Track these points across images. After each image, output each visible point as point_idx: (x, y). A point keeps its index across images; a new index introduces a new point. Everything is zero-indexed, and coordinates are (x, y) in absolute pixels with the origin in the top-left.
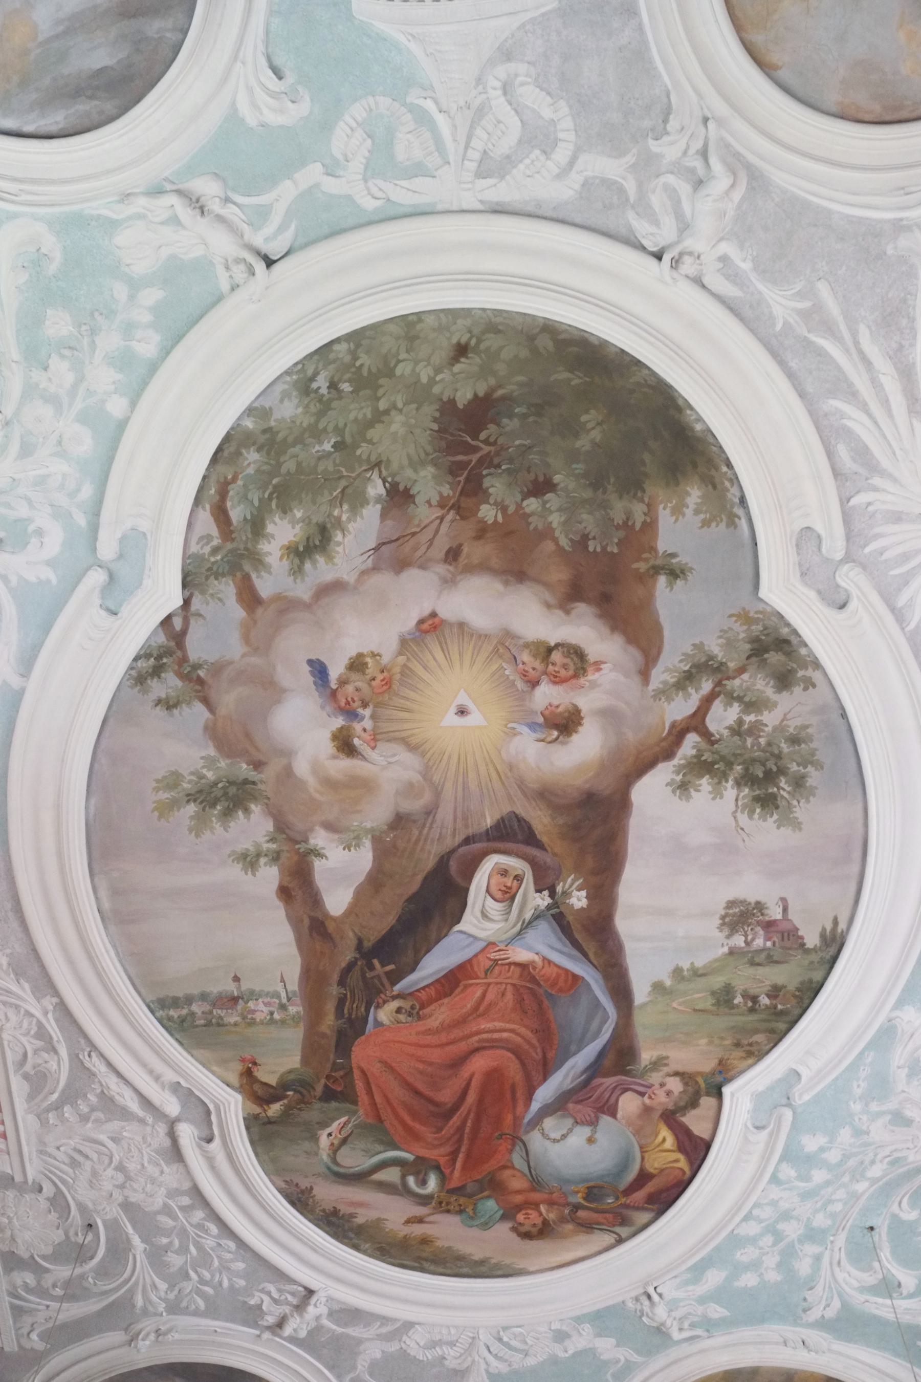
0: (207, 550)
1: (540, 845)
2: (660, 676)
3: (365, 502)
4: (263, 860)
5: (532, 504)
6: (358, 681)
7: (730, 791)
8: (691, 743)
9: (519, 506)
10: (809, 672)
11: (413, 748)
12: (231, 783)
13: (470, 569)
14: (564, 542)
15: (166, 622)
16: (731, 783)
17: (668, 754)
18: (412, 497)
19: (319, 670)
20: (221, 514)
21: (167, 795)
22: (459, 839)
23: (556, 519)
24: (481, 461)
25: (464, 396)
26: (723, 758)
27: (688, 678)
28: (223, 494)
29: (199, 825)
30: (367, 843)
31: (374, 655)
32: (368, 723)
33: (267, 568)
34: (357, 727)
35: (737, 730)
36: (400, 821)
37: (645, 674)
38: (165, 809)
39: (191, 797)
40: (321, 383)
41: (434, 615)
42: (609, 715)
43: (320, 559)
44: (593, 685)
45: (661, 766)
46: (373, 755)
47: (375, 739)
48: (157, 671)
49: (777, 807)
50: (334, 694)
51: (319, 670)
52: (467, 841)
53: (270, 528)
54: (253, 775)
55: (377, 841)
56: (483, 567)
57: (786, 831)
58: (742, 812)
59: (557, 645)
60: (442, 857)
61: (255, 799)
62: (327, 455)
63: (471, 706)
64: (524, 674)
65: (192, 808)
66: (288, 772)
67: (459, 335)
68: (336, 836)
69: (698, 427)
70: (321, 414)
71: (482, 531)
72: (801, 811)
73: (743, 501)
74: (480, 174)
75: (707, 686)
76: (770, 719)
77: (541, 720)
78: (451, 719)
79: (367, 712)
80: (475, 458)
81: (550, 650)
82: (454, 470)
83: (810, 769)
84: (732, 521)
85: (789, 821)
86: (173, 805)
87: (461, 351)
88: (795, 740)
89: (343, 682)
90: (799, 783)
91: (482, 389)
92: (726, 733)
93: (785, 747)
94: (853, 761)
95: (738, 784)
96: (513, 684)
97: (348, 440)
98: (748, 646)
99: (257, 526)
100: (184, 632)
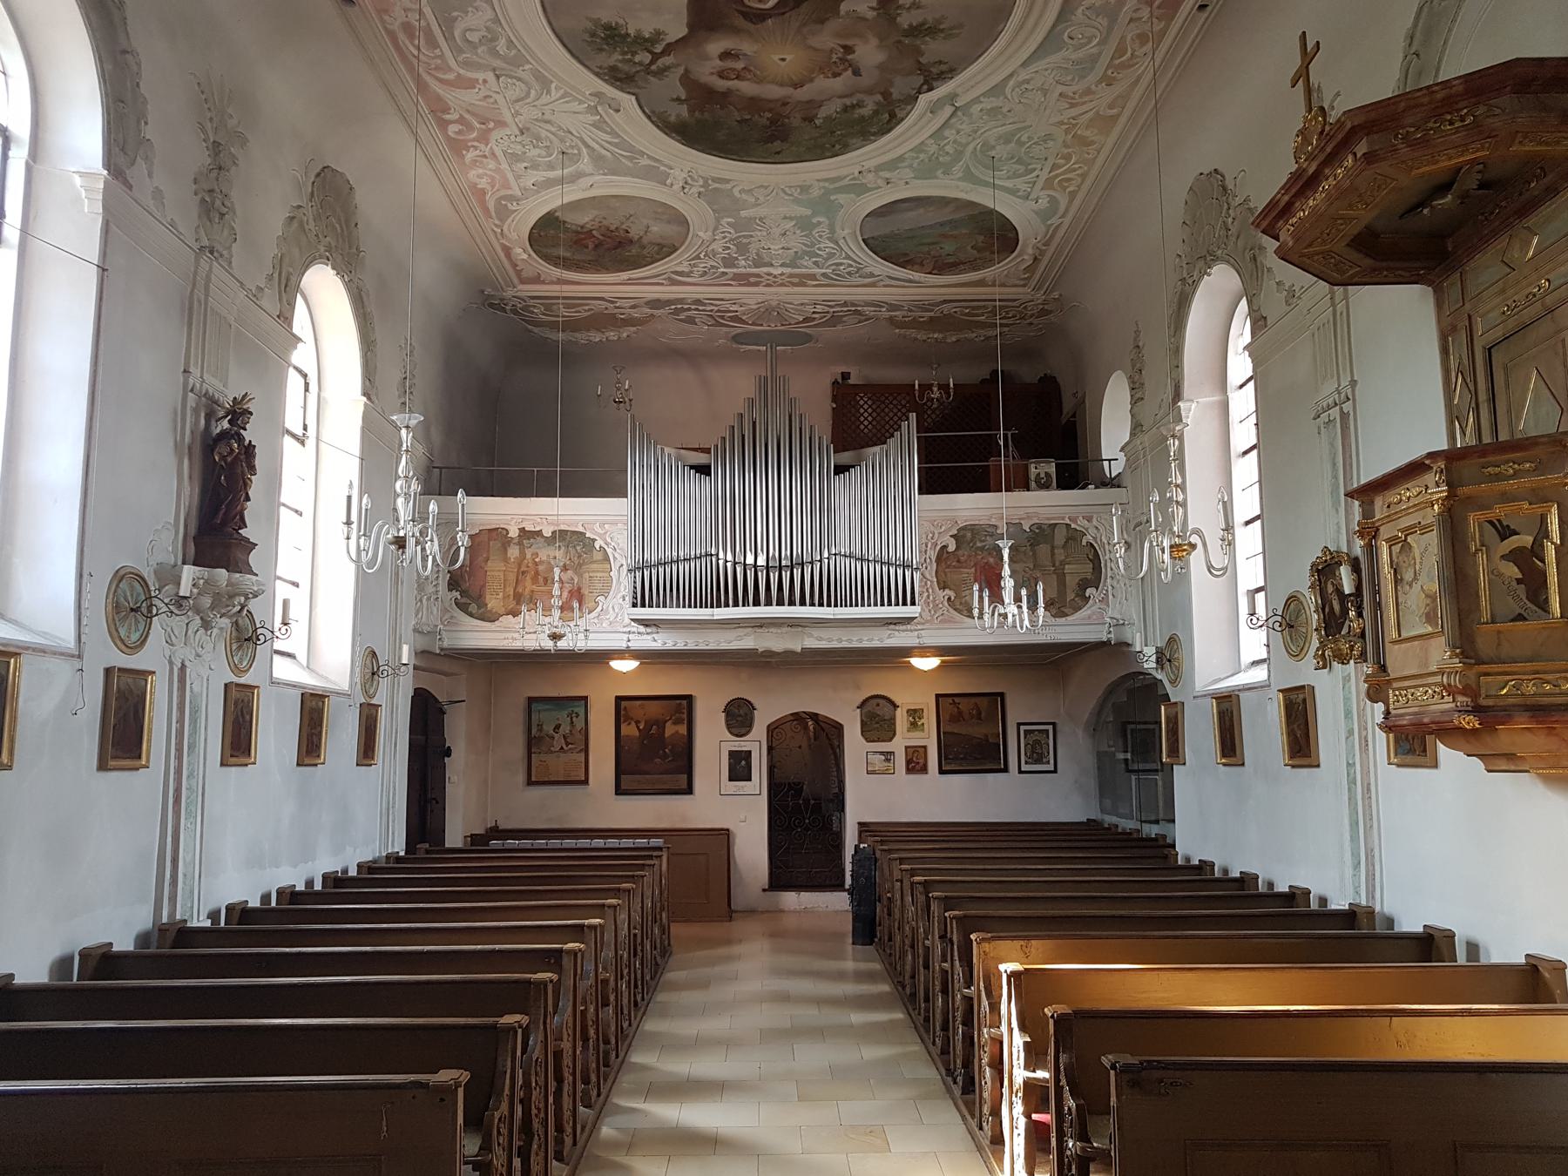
0: (903, 106)
1: (737, 10)
2: (681, 70)
3: (824, 118)
4: (907, 6)
5: (748, 117)
6: (837, 70)
7: (632, 32)
8: (659, 49)
9: (753, 116)
10: (601, 71)
11: (810, 47)
12: (914, 36)
13: (777, 100)
14: (732, 107)
15: (930, 89)
16: (632, 35)
17: (669, 45)
18: (802, 118)
19: (857, 73)
20: (892, 115)
21: (954, 31)
22: (787, 15)
23: (736, 113)
24: (770, 127)
25: (777, 144)
26: (638, 43)
27: (666, 69)
28: (889, 121)
29: (939, 21)
30: (842, 13)
31: (828, 77)
32: (834, 56)
33: (875, 102)
34: (840, 55)
35: (634, 54)
36: (822, 21)
37: (687, 71)
38: (961, 26)
39: (942, 31)
40: (838, 147)
41: (796, 89)
42: (707, 58)
43: (848, 103)
44: (714, 68)
45: (673, 41)
46: (833, 45)
47: (831, 51)
48: (942, 73)
49: (602, 26)
50: (850, 66)
51: (857, 73)
52: (784, 14)
53: (871, 112)
54: (902, 39)
55: (836, 12)
56: (770, 101)
57: (595, 17)
58: (622, 25)
59: (733, 79)
60: (798, 7)
61: (905, 30)
62: (839, 130)
63: (779, 62)
64: (750, 71)
65: (942, 27)
66: (881, 40)
67: (778, 157)
68: (861, 15)
69: (674, 135)
70: (840, 140)
71: (770, 110)
72: (589, 25)
73: (649, 117)
74: (769, 186)
75: (653, 67)
76: (617, 56)
77: (741, 57)
78: (789, 57)
79: (834, 60)
80: (773, 128)
81: (737, 78)
82: (783, 125)
83: (589, 40)
84: (653, 112)
85: (596, 22)
86: (951, 28)
87: (778, 153)
88: (601, 50)
89: (846, 70)
90: (593, 35)
91: (770, 145)
92: (639, 52)
93: (605, 47)
94: (566, 42)
95: (628, 35)
96: (755, 68)
97: (829, 135)
98: (636, 79)
99: (876, 113)
100: (922, 85)
